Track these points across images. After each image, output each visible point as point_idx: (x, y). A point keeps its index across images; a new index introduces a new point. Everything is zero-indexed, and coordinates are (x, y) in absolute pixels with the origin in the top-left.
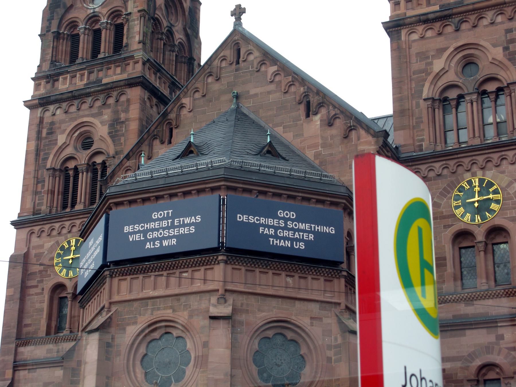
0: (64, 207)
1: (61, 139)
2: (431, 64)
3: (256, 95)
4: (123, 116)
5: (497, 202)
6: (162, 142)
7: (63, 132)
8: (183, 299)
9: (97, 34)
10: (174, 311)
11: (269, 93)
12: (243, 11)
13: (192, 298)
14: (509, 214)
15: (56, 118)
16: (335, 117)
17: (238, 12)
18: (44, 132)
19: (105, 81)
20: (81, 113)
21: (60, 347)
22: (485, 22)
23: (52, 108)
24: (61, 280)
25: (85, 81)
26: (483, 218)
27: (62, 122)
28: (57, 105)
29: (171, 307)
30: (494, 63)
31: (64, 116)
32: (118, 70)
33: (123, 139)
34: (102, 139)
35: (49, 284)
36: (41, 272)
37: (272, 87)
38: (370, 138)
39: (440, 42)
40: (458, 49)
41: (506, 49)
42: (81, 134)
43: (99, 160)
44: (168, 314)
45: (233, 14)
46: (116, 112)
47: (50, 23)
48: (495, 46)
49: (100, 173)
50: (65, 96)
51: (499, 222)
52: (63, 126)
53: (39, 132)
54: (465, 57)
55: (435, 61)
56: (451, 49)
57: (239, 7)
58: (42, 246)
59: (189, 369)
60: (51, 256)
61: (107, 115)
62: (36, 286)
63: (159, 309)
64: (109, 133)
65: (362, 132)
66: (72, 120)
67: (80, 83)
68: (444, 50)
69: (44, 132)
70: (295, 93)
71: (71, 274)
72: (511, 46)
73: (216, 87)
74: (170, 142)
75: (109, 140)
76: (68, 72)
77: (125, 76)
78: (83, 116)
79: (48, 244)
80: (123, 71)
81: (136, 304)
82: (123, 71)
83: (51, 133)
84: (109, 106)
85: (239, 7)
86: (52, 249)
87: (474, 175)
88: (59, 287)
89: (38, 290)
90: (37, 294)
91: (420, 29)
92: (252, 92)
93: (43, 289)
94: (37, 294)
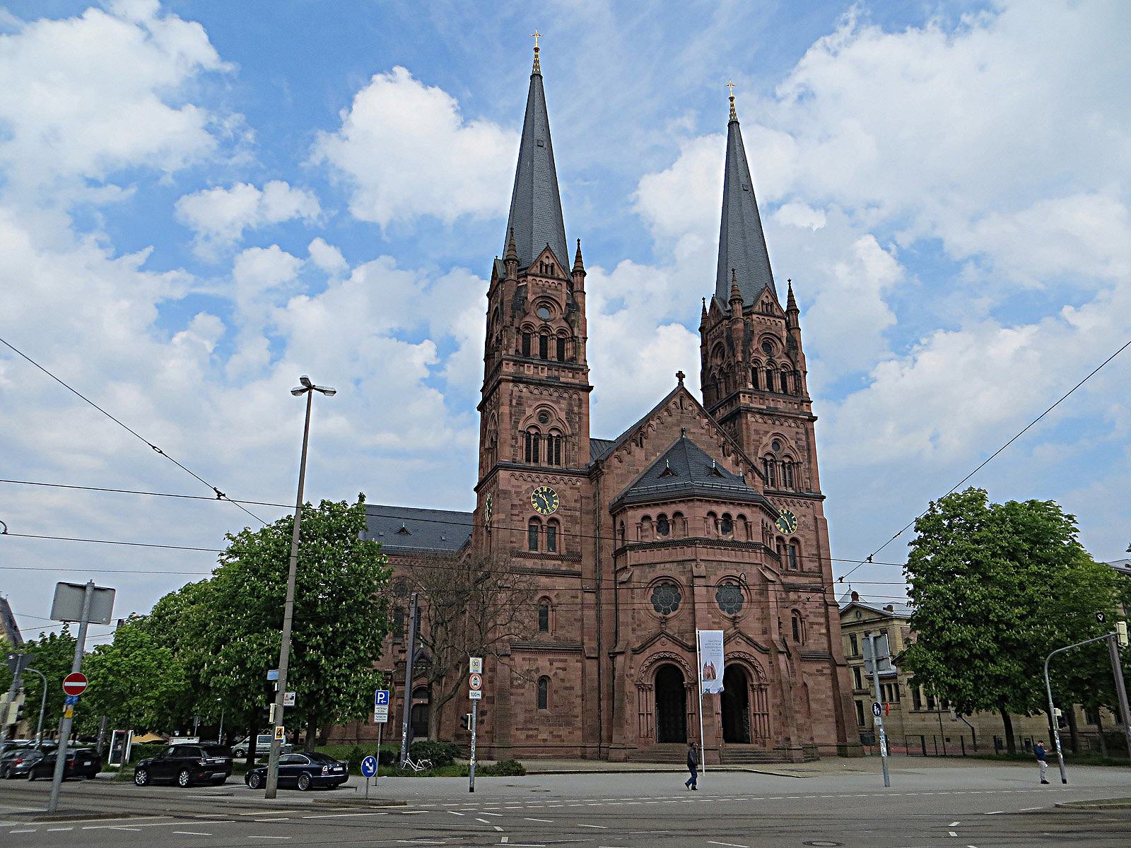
0: (528, 460)
1: (529, 412)
4: (576, 409)
12: (684, 376)
13: (746, 565)
14: (801, 533)
15: (523, 394)
17: (680, 376)
18: (514, 402)
19: (561, 379)
21: (544, 563)
23: (521, 386)
24: (537, 514)
25: (545, 374)
27: (528, 399)
28: (525, 385)
29: (735, 569)
32: (571, 375)
34: (560, 420)
38: (760, 479)
39: (765, 427)
41: (796, 442)
45: (677, 375)
46: (570, 405)
48: (792, 439)
49: (555, 443)
50: (534, 381)
51: (795, 536)
54: (775, 439)
57: (680, 372)
59: (745, 605)
61: (564, 404)
62: (518, 515)
64: (566, 418)
67: (544, 374)
68: (767, 432)
69: (514, 402)
73: (670, 419)
76: (532, 363)
77: (577, 381)
79: (525, 487)
80: (573, 377)
81: (715, 563)
82: (573, 377)
83: (519, 404)
84: (565, 399)
85: (680, 372)
86: (527, 491)
88: (535, 518)
90: (518, 521)
93: (523, 518)
94: (518, 521)
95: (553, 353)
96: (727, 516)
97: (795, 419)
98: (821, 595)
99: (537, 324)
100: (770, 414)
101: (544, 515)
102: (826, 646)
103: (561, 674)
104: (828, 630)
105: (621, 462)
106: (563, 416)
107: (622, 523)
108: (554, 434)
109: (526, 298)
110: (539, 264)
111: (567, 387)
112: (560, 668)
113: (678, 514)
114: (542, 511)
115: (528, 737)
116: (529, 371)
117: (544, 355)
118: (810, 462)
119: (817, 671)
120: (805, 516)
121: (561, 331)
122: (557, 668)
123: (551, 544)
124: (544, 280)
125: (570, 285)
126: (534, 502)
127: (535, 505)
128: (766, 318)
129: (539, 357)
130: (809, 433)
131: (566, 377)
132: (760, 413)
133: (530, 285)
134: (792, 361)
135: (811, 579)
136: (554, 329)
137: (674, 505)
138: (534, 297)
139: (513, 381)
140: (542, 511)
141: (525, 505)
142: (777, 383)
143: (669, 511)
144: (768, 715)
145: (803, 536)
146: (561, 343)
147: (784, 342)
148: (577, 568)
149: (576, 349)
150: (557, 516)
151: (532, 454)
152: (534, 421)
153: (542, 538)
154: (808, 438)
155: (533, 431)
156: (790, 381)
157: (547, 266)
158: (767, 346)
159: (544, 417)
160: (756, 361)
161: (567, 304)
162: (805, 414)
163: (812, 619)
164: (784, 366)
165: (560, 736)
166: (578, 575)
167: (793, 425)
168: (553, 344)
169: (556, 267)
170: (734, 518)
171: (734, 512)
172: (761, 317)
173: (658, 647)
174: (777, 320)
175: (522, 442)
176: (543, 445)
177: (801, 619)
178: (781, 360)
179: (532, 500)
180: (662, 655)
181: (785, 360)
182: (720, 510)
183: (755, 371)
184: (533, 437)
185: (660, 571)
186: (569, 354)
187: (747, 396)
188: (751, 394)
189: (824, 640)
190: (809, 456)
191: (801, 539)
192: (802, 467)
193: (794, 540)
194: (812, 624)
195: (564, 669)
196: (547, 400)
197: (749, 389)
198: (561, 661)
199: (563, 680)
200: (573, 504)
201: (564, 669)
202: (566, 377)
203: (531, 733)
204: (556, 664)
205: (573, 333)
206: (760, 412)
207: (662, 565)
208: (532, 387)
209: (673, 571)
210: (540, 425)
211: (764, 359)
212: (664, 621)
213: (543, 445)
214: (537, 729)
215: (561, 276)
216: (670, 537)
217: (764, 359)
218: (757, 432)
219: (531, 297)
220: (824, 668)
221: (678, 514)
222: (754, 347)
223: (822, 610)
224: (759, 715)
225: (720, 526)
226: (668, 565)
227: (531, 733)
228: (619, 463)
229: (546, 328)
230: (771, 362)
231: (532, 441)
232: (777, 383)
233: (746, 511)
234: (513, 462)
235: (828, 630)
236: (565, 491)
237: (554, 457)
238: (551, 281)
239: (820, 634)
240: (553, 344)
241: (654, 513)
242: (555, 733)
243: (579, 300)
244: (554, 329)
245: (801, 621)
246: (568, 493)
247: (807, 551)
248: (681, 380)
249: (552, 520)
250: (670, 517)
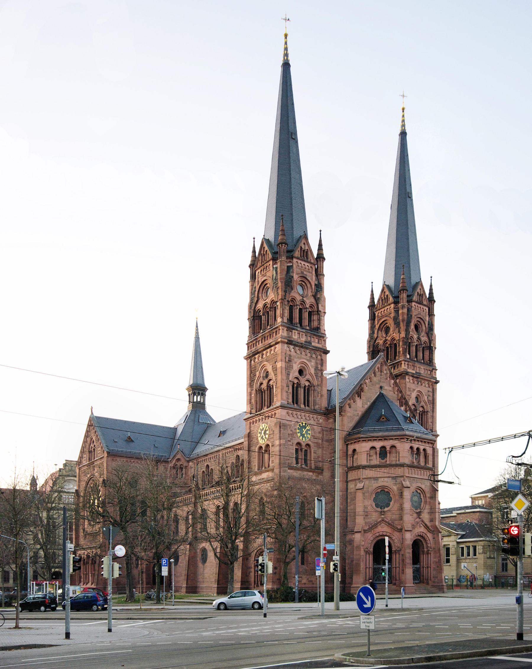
2: (411, 394)
19: (313, 344)
23: (292, 347)
34: (310, 374)
61: (313, 363)
68: (414, 390)
82: (318, 343)
95: (306, 322)
99: (299, 298)
100: (417, 377)
106: (313, 371)
109: (293, 277)
111: (317, 349)
116: (295, 336)
121: (311, 306)
130: (434, 391)
132: (413, 376)
133: (294, 266)
139: (287, 343)
142: (420, 355)
146: (310, 314)
149: (319, 320)
168: (306, 315)
186: (315, 324)
187: (406, 363)
205: (318, 308)
210: (300, 377)
229: (303, 302)
232: (420, 355)
240: (306, 315)
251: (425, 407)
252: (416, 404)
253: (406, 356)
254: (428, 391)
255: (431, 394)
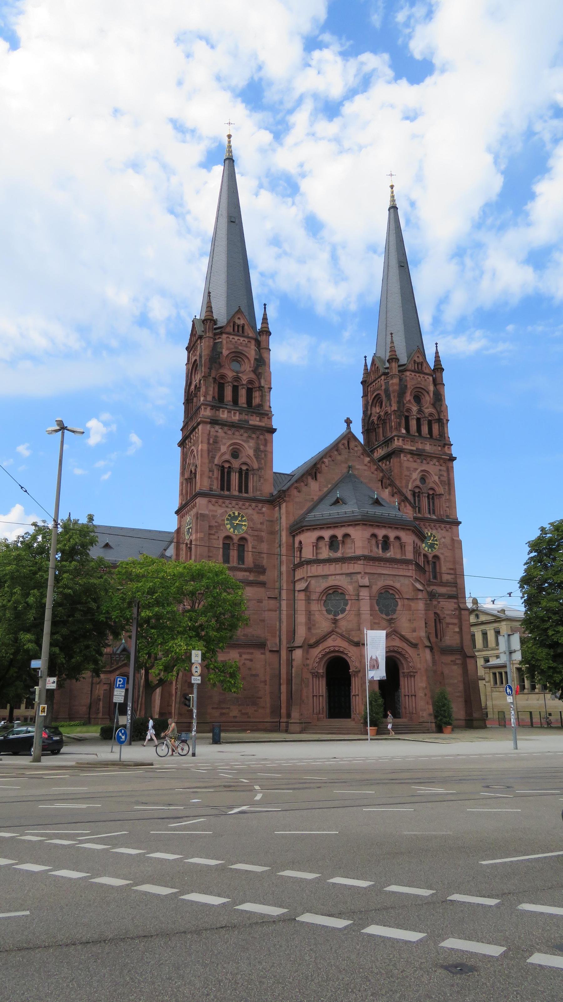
0: (222, 489)
1: (223, 449)
2: (411, 474)
3: (358, 469)
4: (262, 447)
5: (437, 544)
6: (313, 479)
7: (225, 444)
8: (397, 577)
9: (235, 390)
10: (394, 582)
11: (365, 470)
14: (441, 551)
15: (218, 434)
16: (396, 493)
17: (348, 422)
19: (251, 422)
20: (235, 436)
22: (432, 463)
23: (217, 427)
26: (432, 551)
28: (220, 427)
29: (392, 580)
30: (434, 482)
31: (224, 435)
32: (258, 419)
33: (263, 461)
34: (248, 456)
35: (222, 535)
36: (216, 526)
37: (366, 468)
38: (410, 508)
39: (414, 465)
40: (422, 471)
41: (439, 478)
42: (233, 449)
43: (244, 468)
44: (390, 583)
46: (258, 444)
47: (210, 371)
48: (436, 475)
50: (228, 424)
51: (437, 554)
52: (224, 441)
53: (209, 440)
55: (413, 474)
56: (419, 470)
57: (348, 419)
58: (216, 511)
60: (223, 518)
61: (252, 443)
62: (214, 535)
63: (387, 580)
64: (254, 455)
65: (408, 504)
66: (229, 439)
67: (236, 418)
68: (417, 469)
69: (211, 441)
70: (377, 475)
71: (236, 531)
72: (441, 477)
73: (339, 458)
74: (316, 479)
75: (255, 459)
76: (226, 408)
77: (262, 424)
78: (236, 439)
80: (260, 421)
81: (376, 576)
82: (260, 421)
84: (253, 438)
85: (348, 419)
86: (222, 515)
87: (429, 531)
88: (228, 537)
89: (215, 537)
90: (215, 539)
91: (409, 456)
92: (357, 467)
93: (218, 537)
94: (215, 539)
95: (243, 399)
96: (386, 538)
97: (439, 459)
98: (456, 601)
99: (230, 375)
100: (419, 455)
101: (236, 534)
102: (458, 641)
103: (248, 663)
104: (461, 629)
105: (299, 492)
106: (251, 452)
107: (300, 543)
108: (244, 468)
109: (222, 353)
110: (232, 325)
111: (255, 429)
112: (248, 660)
113: (346, 536)
114: (234, 532)
115: (222, 714)
116: (223, 415)
117: (235, 401)
118: (450, 494)
119: (452, 661)
120: (444, 538)
121: (250, 382)
122: (246, 659)
123: (241, 558)
124: (236, 338)
125: (258, 343)
126: (227, 524)
127: (228, 526)
128: (418, 375)
129: (231, 403)
130: (449, 470)
131: (255, 421)
133: (224, 342)
134: (437, 410)
135: (449, 588)
136: (245, 379)
137: (343, 528)
138: (228, 352)
139: (210, 423)
140: (234, 532)
141: (220, 526)
142: (425, 429)
143: (339, 533)
144: (415, 696)
145: (442, 554)
146: (250, 392)
147: (432, 394)
148: (262, 578)
149: (262, 397)
150: (246, 536)
151: (225, 484)
152: (227, 457)
153: (234, 554)
154: (448, 474)
155: (227, 465)
156: (435, 427)
157: (238, 326)
158: (418, 399)
159: (235, 454)
160: (409, 410)
161: (256, 359)
162: (446, 454)
163: (448, 620)
164: (431, 414)
165: (247, 714)
166: (263, 584)
167: (437, 464)
168: (243, 393)
169: (246, 327)
170: (392, 539)
171: (392, 534)
172: (413, 374)
173: (330, 643)
174: (426, 377)
175: (217, 474)
176: (235, 478)
177: (439, 620)
178: (428, 410)
179: (226, 522)
180: (332, 649)
181: (431, 410)
182: (381, 533)
183: (407, 419)
184: (226, 470)
185: (331, 582)
186: (256, 401)
187: (401, 439)
188: (404, 437)
189: (457, 637)
190: (449, 489)
191: (441, 556)
192: (444, 498)
193: (436, 557)
194: (448, 624)
195: (251, 660)
196: (240, 440)
197: (403, 433)
198: (248, 653)
199: (250, 669)
200: (259, 526)
201: (251, 660)
202: (255, 421)
203: (224, 711)
204: (245, 656)
205: (260, 383)
206: (411, 453)
207: (333, 577)
208: (226, 428)
209: (342, 582)
210: (233, 461)
211: (415, 409)
212: (335, 622)
213: (235, 478)
214: (229, 708)
215: (251, 335)
216: (388, 555)
217: (415, 409)
218: (408, 469)
219: (225, 352)
220: (456, 659)
221: (346, 536)
222: (408, 399)
223: (457, 612)
224: (408, 696)
225: (380, 546)
226: (338, 577)
227: (224, 711)
228: (298, 493)
229: (237, 379)
230: (420, 411)
231: (225, 473)
232: (425, 429)
233: (402, 534)
234: (210, 491)
235: (461, 629)
236: (253, 515)
237: (243, 486)
238: (242, 339)
239: (455, 632)
240: (243, 393)
241: (327, 534)
242: (243, 711)
243: (265, 355)
244: (245, 379)
245: (440, 622)
246: (256, 517)
247: (444, 567)
248: (348, 425)
249: (243, 539)
250: (340, 538)
251: (436, 488)
252: (421, 486)
253: (400, 430)
254: (440, 470)
255: (445, 474)
